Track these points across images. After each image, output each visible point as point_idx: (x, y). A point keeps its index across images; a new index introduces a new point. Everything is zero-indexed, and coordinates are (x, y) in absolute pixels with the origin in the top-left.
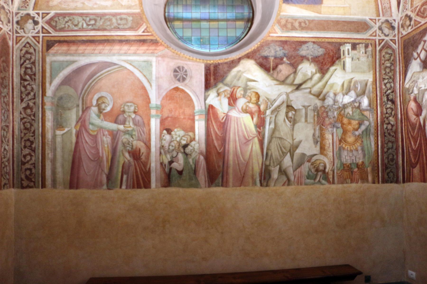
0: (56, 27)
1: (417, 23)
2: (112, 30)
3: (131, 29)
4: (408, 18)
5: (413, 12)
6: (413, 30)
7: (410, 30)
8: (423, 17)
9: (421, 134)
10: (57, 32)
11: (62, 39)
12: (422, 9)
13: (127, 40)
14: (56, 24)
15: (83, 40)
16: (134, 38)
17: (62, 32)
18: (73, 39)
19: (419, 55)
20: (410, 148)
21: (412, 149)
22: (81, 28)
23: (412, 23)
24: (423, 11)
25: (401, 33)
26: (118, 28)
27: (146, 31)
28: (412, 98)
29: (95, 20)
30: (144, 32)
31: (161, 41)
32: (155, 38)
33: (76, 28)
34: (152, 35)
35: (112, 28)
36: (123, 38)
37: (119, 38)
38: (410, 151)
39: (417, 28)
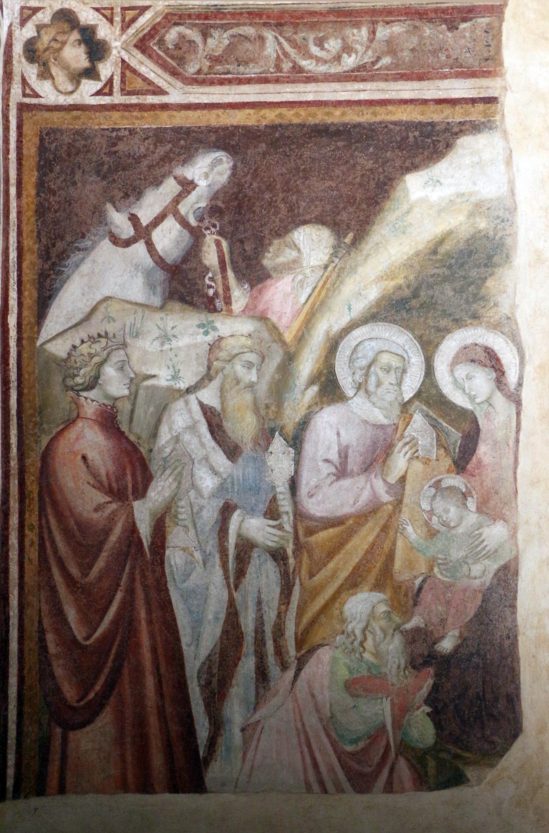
1: (139, 84)
4: (75, 36)
5: (111, 21)
6: (113, 107)
7: (87, 92)
8: (174, 73)
9: (132, 579)
12: (172, 35)
19: (143, 233)
20: (50, 637)
21: (70, 643)
23: (106, 69)
24: (177, 47)
25: (24, 82)
28: (90, 409)
38: (52, 648)
39: (141, 107)
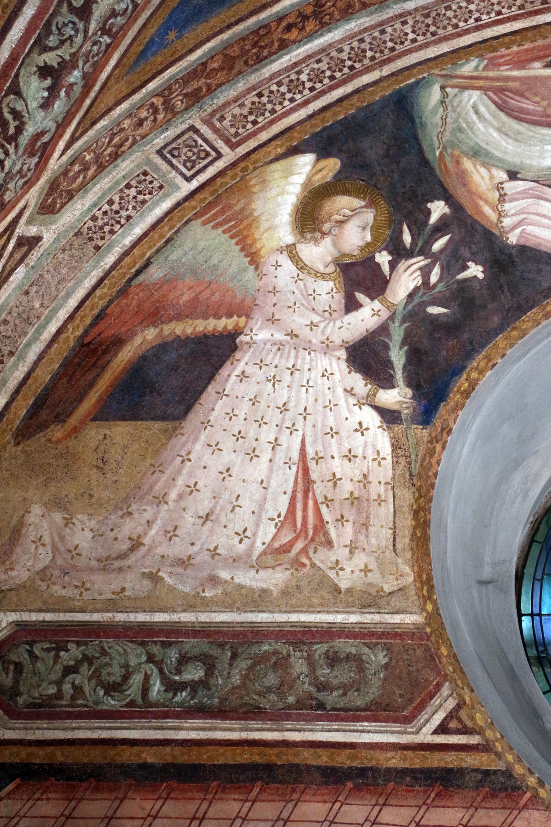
0: (15, 693)
2: (288, 717)
3: (381, 711)
10: (19, 723)
11: (40, 756)
13: (362, 772)
14: (16, 681)
15: (144, 766)
16: (395, 761)
17: (44, 724)
18: (96, 756)
22: (140, 701)
26: (316, 709)
27: (453, 724)
29: (210, 666)
30: (442, 729)
31: (532, 781)
32: (501, 766)
33: (112, 703)
34: (485, 748)
35: (290, 707)
36: (343, 760)
37: (323, 759)
